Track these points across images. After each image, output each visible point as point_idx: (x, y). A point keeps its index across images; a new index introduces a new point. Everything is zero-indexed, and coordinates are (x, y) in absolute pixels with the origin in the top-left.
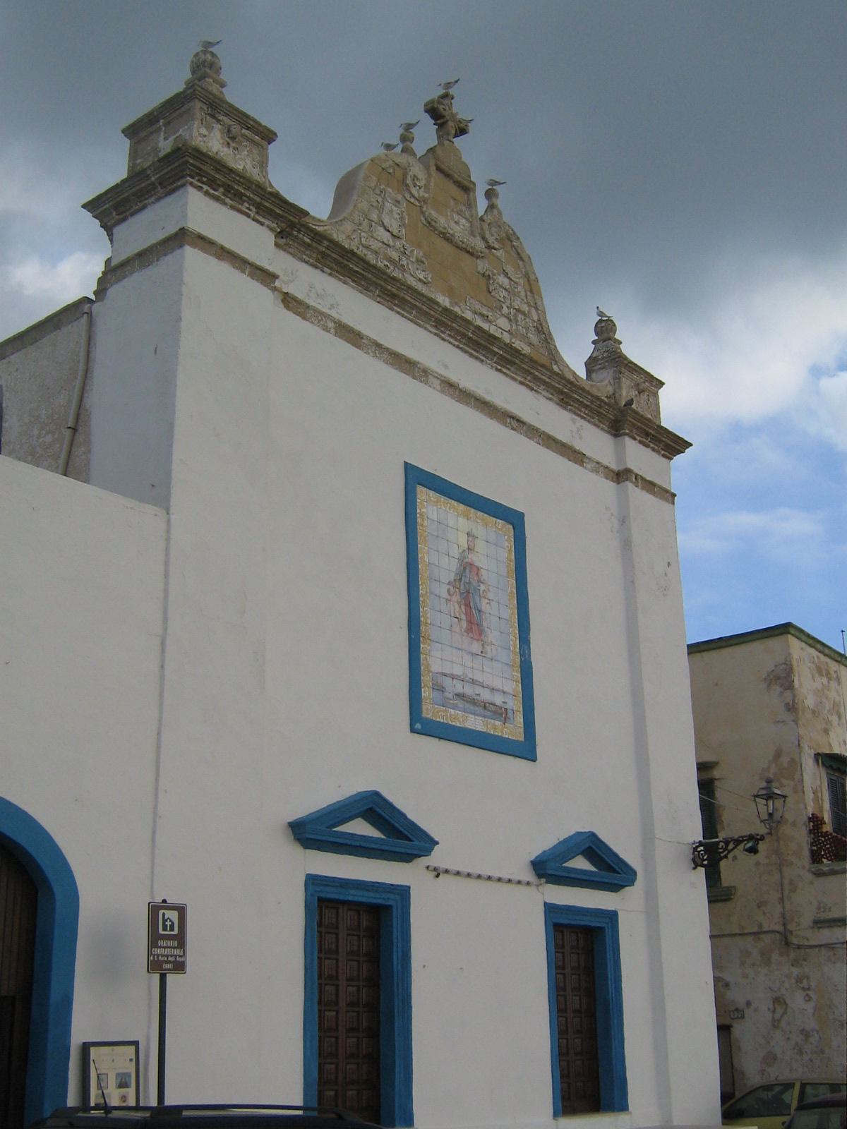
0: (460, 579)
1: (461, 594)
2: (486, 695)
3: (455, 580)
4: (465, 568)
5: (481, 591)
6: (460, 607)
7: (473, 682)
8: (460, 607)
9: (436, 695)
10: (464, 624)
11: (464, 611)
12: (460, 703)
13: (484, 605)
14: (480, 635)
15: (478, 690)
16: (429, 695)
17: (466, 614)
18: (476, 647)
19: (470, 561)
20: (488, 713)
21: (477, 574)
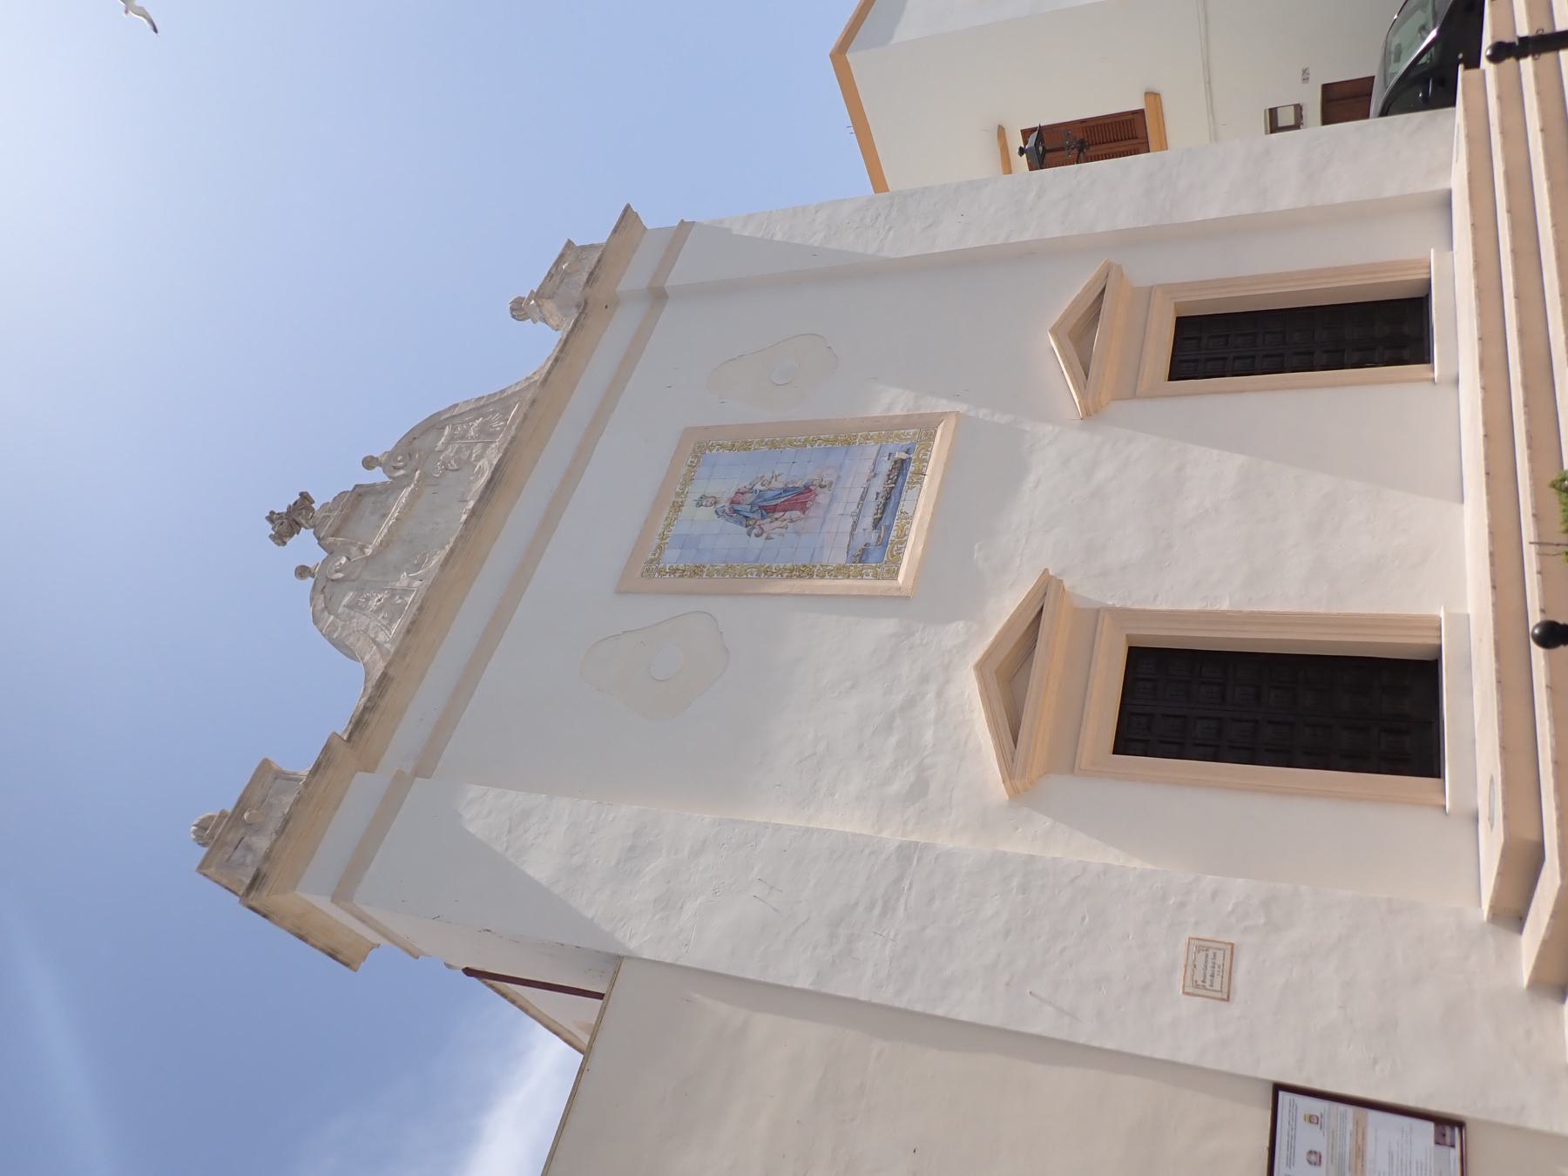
0: (746, 517)
1: (763, 517)
2: (879, 485)
3: (747, 526)
4: (736, 511)
5: (762, 488)
6: (777, 519)
7: (862, 498)
8: (777, 519)
9: (875, 554)
10: (796, 514)
11: (781, 514)
12: (884, 524)
13: (778, 484)
14: (811, 491)
15: (872, 496)
16: (871, 567)
17: (785, 511)
18: (822, 498)
19: (727, 504)
20: (900, 479)
21: (742, 493)
